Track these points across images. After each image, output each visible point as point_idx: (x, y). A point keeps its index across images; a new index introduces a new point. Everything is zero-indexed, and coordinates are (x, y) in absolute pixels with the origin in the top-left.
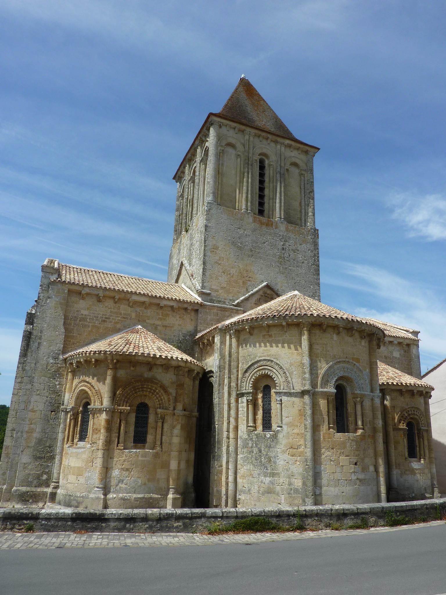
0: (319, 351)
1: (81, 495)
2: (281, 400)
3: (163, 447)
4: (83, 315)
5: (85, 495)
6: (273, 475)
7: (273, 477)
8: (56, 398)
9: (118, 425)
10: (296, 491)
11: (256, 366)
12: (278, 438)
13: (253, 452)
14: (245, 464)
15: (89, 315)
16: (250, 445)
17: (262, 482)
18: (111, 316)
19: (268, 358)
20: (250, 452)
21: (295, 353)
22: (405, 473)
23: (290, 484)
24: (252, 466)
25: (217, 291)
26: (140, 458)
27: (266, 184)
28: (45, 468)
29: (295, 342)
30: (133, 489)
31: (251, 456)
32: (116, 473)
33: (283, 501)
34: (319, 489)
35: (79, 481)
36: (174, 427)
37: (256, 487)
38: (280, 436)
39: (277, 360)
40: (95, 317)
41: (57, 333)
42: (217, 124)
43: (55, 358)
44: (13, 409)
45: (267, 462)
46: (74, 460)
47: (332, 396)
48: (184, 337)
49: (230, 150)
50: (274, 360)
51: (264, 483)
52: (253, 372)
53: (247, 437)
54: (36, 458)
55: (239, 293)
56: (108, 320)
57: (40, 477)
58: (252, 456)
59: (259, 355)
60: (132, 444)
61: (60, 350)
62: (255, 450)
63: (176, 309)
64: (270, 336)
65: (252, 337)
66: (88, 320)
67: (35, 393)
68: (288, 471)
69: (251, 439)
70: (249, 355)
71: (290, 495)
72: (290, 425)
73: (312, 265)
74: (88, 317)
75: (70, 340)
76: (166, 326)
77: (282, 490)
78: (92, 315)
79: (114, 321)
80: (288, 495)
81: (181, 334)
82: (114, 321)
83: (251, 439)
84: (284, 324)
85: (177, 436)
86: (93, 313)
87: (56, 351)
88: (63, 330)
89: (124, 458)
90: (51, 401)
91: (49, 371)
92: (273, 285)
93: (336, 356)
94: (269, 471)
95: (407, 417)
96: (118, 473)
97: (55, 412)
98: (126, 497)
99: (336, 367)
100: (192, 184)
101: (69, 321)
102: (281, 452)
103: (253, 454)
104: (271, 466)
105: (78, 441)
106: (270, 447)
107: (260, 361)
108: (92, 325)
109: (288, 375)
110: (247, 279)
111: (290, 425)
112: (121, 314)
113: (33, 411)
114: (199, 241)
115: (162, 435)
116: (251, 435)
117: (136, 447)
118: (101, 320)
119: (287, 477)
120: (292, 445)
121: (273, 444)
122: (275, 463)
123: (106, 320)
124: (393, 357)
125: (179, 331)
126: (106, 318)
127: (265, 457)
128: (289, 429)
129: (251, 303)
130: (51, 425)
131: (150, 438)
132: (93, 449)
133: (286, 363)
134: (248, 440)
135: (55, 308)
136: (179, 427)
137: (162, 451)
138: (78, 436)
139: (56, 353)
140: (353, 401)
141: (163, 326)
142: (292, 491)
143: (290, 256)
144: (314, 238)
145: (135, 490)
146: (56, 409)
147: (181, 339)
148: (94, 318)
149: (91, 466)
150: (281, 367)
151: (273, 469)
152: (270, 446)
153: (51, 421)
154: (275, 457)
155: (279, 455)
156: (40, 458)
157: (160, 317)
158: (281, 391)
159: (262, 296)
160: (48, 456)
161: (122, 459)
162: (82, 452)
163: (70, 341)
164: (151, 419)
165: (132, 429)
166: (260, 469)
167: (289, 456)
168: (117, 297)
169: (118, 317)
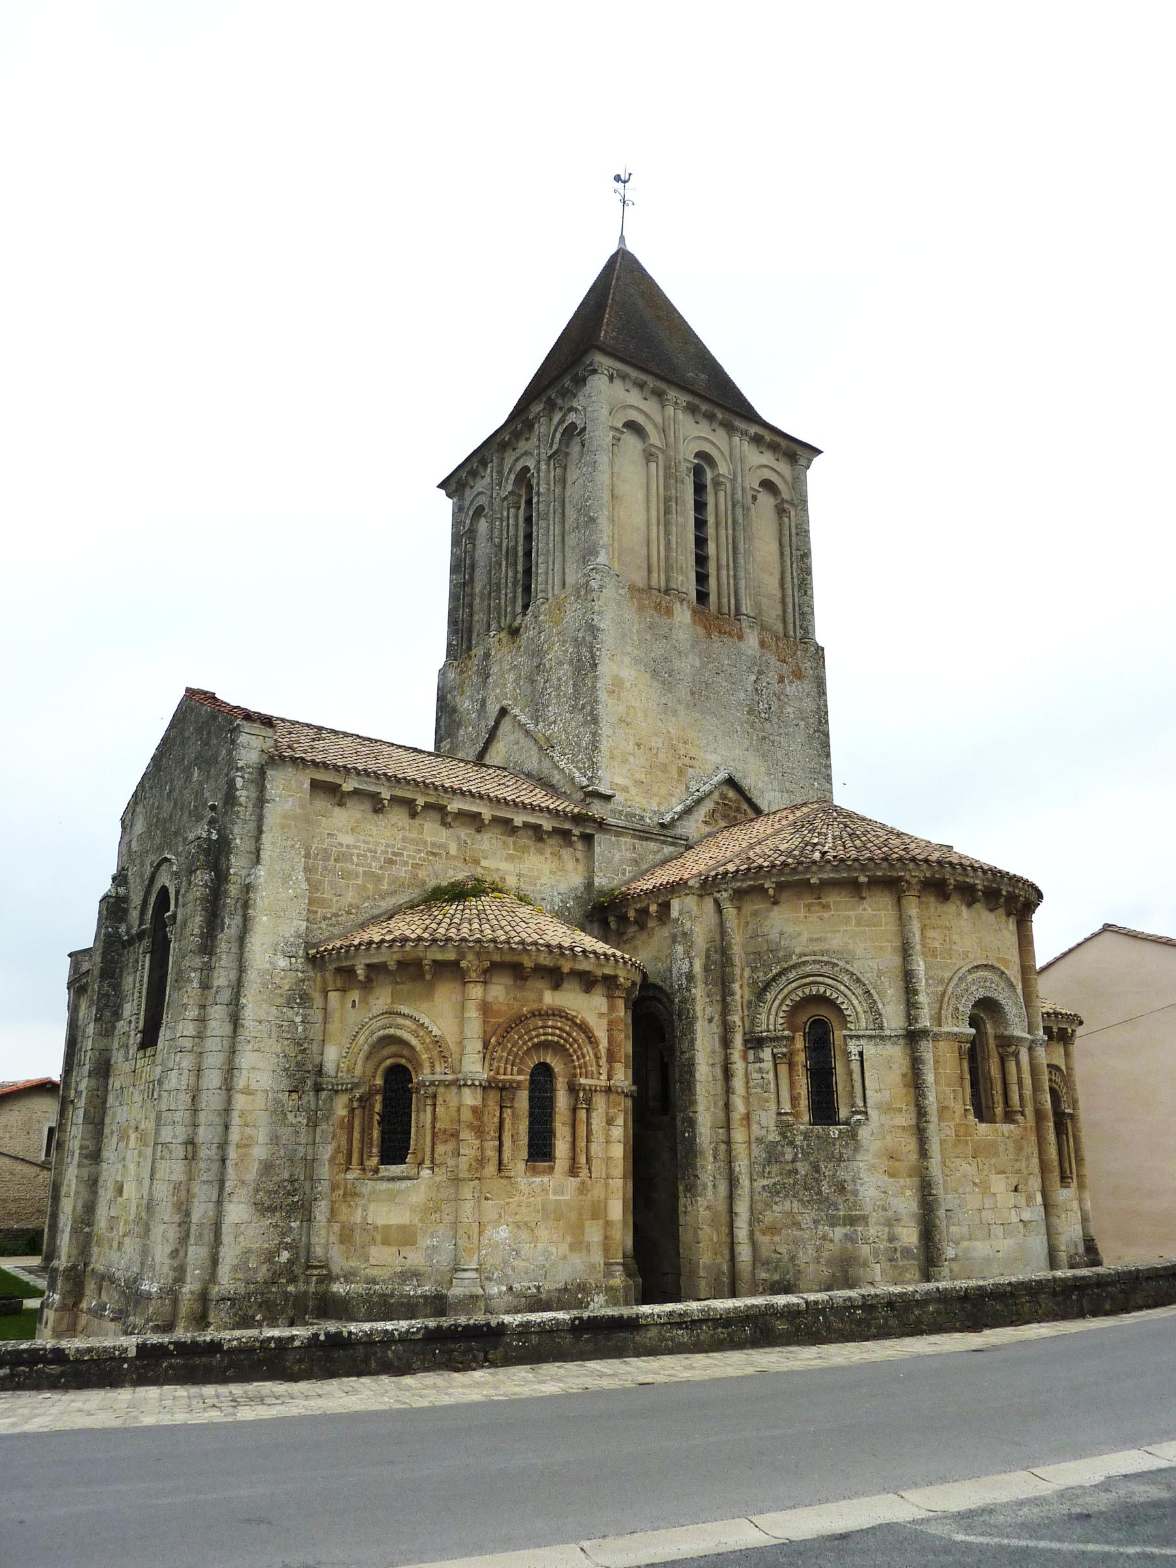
0: (937, 944)
2: (861, 1054)
3: (593, 1169)
6: (851, 1221)
7: (851, 1225)
9: (496, 1120)
10: (906, 1252)
11: (792, 975)
12: (859, 1138)
13: (797, 1172)
14: (777, 1199)
16: (789, 1157)
17: (824, 1238)
18: (404, 848)
19: (825, 959)
20: (790, 1172)
21: (887, 946)
23: (892, 1238)
24: (795, 1204)
25: (625, 789)
26: (551, 1197)
27: (711, 530)
28: (284, 1235)
29: (887, 923)
31: (792, 1181)
32: (502, 1233)
33: (878, 1278)
35: (405, 1258)
36: (610, 1122)
37: (810, 1251)
38: (864, 1133)
39: (847, 962)
41: (290, 891)
42: (606, 372)
43: (290, 957)
44: (184, 1088)
45: (835, 1192)
46: (385, 1209)
47: (967, 1042)
48: (562, 901)
49: (631, 441)
50: (841, 963)
51: (832, 1241)
52: (786, 991)
53: (778, 1139)
54: (263, 1209)
55: (672, 795)
57: (275, 1257)
58: (795, 1183)
59: (798, 951)
61: (299, 936)
62: (803, 1168)
63: (548, 833)
64: (826, 907)
65: (776, 908)
66: (355, 858)
67: (250, 1047)
68: (886, 1210)
69: (791, 1143)
70: (771, 951)
71: (894, 1263)
72: (887, 1108)
73: (815, 731)
74: (356, 851)
75: (315, 909)
77: (876, 1253)
78: (363, 845)
79: (411, 861)
80: (889, 1264)
81: (556, 894)
82: (411, 861)
83: (791, 1143)
84: (863, 879)
87: (292, 939)
88: (304, 886)
89: (516, 1198)
90: (288, 1066)
91: (278, 991)
92: (737, 777)
93: (970, 955)
94: (842, 1213)
96: (506, 1235)
97: (297, 1092)
99: (970, 978)
100: (512, 510)
101: (312, 861)
102: (868, 1170)
103: (799, 1176)
104: (845, 1201)
105: (378, 1164)
106: (840, 1159)
107: (804, 963)
109: (876, 997)
110: (687, 761)
111: (887, 1108)
112: (425, 843)
113: (248, 1092)
114: (571, 662)
115: (588, 1141)
116: (789, 1134)
117: (535, 1172)
118: (382, 859)
119: (885, 1225)
121: (847, 1153)
122: (855, 1193)
125: (552, 887)
126: (394, 854)
127: (828, 1182)
128: (883, 1117)
129: (697, 821)
130: (292, 1125)
131: (561, 1148)
132: (437, 1179)
133: (868, 969)
134: (782, 1146)
135: (283, 828)
136: (620, 1121)
137: (591, 1177)
138: (375, 1150)
140: (999, 1053)
142: (898, 1255)
143: (770, 708)
144: (816, 668)
147: (557, 908)
148: (369, 854)
149: (438, 1220)
150: (858, 978)
151: (850, 1208)
152: (841, 1157)
153: (290, 1116)
154: (853, 1181)
155: (861, 1176)
156: (272, 1209)
158: (861, 1033)
159: (718, 803)
160: (288, 1205)
163: (316, 912)
164: (562, 1100)
165: (524, 1126)
166: (819, 1209)
167: (886, 1178)
168: (420, 801)
169: (420, 851)
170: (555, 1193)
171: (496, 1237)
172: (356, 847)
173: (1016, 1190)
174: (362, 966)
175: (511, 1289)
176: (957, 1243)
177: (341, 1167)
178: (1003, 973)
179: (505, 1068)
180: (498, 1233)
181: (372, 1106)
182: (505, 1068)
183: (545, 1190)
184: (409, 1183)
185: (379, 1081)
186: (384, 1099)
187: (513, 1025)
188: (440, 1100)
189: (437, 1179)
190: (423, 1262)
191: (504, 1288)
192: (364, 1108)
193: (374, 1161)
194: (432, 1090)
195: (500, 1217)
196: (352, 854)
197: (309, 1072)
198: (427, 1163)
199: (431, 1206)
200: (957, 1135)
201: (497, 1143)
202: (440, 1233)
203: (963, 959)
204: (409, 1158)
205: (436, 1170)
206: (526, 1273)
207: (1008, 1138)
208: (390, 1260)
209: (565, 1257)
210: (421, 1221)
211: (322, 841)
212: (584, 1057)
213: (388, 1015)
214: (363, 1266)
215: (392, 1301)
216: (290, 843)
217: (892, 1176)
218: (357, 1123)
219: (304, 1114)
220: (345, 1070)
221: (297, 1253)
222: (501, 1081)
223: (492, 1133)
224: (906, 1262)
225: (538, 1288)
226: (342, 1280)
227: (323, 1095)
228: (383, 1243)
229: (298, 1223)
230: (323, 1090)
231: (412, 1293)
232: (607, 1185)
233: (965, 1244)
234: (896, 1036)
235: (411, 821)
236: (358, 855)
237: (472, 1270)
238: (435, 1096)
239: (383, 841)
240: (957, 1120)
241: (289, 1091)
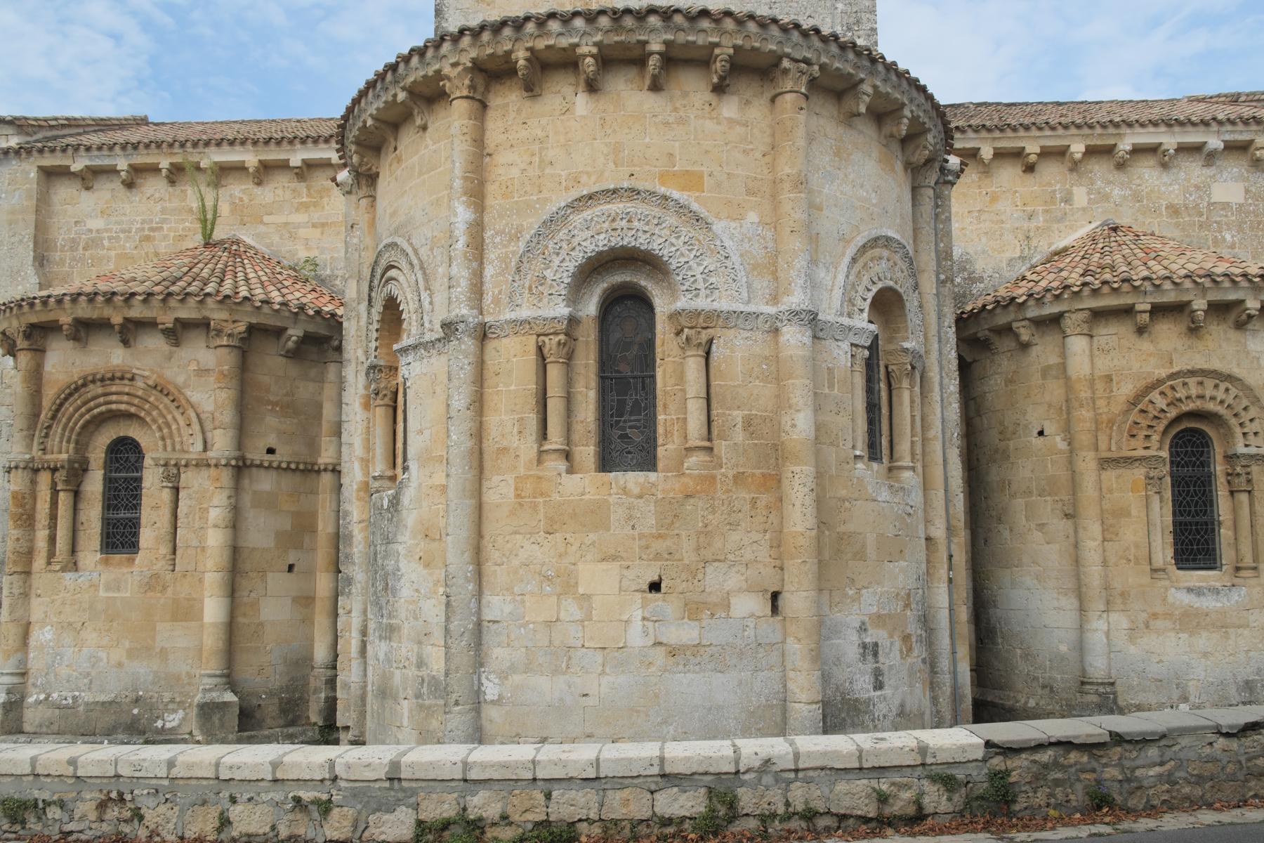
4: (90, 231)
15: (107, 230)
18: (164, 221)
22: (1147, 627)
23: (421, 664)
26: (102, 594)
30: (85, 678)
32: (46, 635)
34: (497, 681)
40: (123, 231)
41: (20, 287)
47: (556, 334)
56: (156, 234)
60: (99, 556)
66: (106, 243)
71: (420, 701)
74: (105, 235)
76: (323, 225)
79: (172, 234)
85: (216, 526)
86: (117, 223)
89: (61, 595)
93: (584, 179)
95: (1163, 411)
101: (59, 253)
108: (117, 255)
118: (137, 238)
120: (428, 529)
123: (152, 234)
124: (1210, 204)
126: (152, 229)
135: (11, 224)
137: (173, 571)
141: (314, 226)
145: (91, 682)
157: (304, 200)
164: (151, 479)
170: (108, 589)
172: (107, 230)
173: (655, 587)
176: (503, 676)
178: (665, 198)
180: (43, 633)
183: (94, 586)
196: (102, 239)
200: (518, 496)
203: (567, 189)
206: (68, 681)
207: (640, 497)
209: (120, 665)
211: (69, 230)
216: (16, 239)
217: (427, 565)
224: (433, 702)
225: (75, 698)
233: (517, 678)
234: (439, 340)
235: (170, 189)
236: (110, 238)
237: (7, 674)
239: (139, 218)
240: (522, 471)
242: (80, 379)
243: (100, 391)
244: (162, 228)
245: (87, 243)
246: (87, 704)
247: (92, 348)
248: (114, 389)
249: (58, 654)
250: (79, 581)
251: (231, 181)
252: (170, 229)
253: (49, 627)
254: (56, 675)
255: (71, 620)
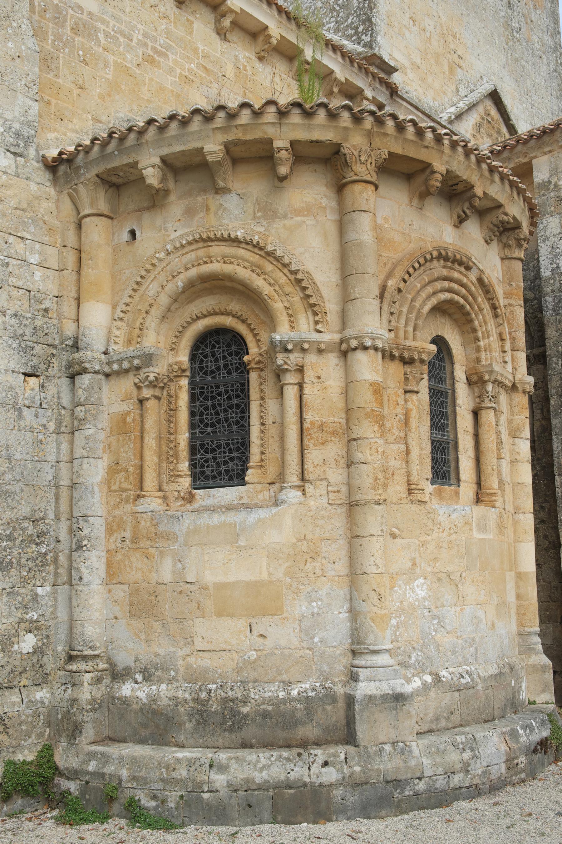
1: (295, 693)
5: (313, 689)
8: (39, 322)
30: (471, 646)
32: (418, 591)
87: (17, 126)
89: (435, 535)
97: (37, 376)
98: (463, 677)
138: (184, 466)
139: (18, 135)
146: (42, 366)
149: (318, 571)
161: (429, 538)
162: (260, 520)
171: (411, 597)
172: (103, 22)
174: (156, 160)
175: (437, 679)
177: (124, 495)
179: (406, 332)
180: (413, 590)
181: (172, 398)
182: (406, 332)
184: (263, 513)
185: (184, 358)
186: (192, 384)
187: (417, 265)
188: (309, 376)
189: (312, 503)
190: (295, 641)
191: (429, 679)
192: (159, 399)
193: (186, 482)
194: (294, 358)
195: (414, 564)
197: (55, 347)
198: (293, 479)
199: (304, 548)
201: (403, 447)
202: (323, 593)
204: (250, 475)
205: (309, 488)
206: (454, 653)
208: (234, 642)
210: (289, 573)
212: (488, 337)
213: (200, 245)
214: (180, 653)
215: (245, 710)
218: (150, 422)
219: (49, 413)
220: (121, 340)
221: (48, 637)
222: (408, 349)
223: (395, 430)
226: (139, 677)
227: (85, 380)
228: (220, 614)
229: (48, 588)
230: (85, 371)
231: (282, 694)
232: (515, 523)
235: (176, 10)
238: (301, 370)
241: (26, 375)
242: (434, 249)
243: (445, 272)
244: (167, 56)
245: (76, 24)
246: (484, 680)
247: (428, 214)
248: (456, 275)
249: (435, 617)
250: (454, 516)
251: (235, 39)
252: (175, 61)
253: (421, 580)
254: (437, 646)
255: (450, 569)
